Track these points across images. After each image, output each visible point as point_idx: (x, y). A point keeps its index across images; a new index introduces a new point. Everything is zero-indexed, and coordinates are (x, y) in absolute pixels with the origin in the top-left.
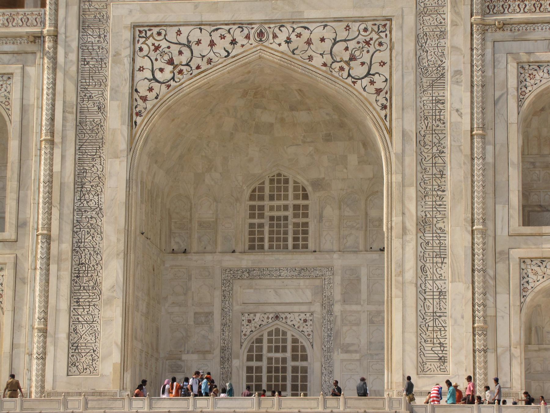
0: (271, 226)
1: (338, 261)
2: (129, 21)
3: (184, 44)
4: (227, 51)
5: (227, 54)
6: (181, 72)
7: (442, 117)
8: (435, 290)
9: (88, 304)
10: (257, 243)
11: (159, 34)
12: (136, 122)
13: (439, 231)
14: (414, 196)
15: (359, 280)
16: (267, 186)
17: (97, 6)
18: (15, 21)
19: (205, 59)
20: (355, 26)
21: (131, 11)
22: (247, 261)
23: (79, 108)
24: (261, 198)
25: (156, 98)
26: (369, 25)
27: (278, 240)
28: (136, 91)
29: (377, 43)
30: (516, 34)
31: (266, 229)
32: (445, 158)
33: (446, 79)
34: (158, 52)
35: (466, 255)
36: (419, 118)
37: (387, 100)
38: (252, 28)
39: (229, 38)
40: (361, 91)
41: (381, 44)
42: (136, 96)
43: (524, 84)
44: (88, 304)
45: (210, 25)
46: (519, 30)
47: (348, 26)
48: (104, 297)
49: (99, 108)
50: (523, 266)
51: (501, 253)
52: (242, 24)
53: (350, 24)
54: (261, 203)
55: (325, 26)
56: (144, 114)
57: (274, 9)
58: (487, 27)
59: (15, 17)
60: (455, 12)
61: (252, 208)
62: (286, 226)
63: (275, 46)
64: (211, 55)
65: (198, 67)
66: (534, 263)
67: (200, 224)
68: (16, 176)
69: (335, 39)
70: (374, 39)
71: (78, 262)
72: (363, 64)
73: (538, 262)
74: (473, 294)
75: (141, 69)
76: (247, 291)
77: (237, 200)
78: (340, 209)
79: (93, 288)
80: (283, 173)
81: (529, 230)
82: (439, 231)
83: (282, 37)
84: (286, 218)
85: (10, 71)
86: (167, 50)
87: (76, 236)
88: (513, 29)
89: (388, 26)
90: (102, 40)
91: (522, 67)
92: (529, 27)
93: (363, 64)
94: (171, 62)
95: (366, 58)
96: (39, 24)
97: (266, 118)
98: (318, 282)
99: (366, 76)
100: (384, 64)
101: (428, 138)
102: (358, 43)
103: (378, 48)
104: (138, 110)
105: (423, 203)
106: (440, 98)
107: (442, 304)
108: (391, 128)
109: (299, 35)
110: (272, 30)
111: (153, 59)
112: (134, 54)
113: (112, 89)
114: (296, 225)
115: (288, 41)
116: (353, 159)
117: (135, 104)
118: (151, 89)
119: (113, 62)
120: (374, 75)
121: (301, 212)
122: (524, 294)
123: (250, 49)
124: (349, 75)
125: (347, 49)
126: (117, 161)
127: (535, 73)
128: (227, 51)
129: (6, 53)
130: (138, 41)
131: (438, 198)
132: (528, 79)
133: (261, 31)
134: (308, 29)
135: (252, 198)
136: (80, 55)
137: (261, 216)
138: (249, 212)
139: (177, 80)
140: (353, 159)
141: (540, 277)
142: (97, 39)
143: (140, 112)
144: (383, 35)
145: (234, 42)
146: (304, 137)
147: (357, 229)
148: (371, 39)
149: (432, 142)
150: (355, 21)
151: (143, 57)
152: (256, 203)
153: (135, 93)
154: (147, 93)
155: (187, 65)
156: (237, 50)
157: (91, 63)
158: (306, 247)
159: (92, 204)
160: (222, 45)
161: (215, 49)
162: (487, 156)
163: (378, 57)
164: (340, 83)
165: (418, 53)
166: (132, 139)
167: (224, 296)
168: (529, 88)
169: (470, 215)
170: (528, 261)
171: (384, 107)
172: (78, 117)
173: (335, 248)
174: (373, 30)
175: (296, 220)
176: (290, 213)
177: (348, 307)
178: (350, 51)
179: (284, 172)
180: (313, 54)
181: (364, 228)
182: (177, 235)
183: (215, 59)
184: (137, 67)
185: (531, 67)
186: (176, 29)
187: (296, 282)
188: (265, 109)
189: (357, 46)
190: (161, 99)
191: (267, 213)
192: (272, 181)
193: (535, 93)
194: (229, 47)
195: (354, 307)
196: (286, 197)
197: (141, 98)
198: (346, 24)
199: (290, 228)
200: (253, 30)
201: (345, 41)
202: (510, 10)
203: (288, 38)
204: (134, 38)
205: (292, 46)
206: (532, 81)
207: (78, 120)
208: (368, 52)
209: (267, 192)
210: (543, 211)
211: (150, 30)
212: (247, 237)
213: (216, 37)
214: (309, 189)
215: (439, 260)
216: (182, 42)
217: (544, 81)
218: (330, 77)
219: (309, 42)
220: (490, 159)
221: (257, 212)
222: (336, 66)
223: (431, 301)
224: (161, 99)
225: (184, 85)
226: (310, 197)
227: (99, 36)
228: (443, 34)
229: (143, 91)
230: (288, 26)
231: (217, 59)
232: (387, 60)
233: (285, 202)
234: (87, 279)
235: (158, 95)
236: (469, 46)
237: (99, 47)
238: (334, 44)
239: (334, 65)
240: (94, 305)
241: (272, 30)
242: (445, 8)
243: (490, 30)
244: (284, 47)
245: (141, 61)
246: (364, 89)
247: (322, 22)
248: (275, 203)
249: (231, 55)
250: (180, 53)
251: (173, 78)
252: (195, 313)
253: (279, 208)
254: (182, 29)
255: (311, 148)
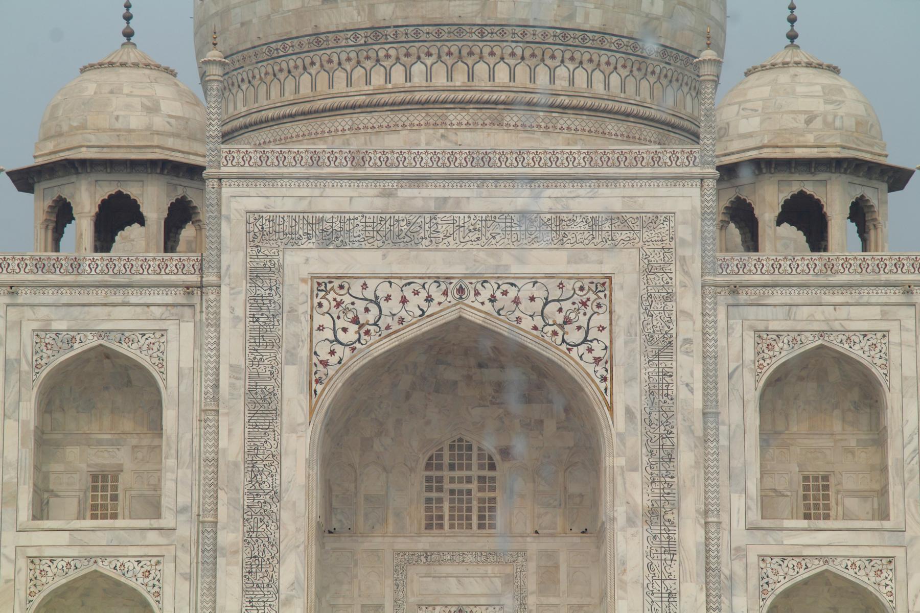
0: (452, 501)
1: (533, 546)
2: (305, 272)
3: (371, 301)
4: (421, 310)
5: (421, 313)
6: (367, 333)
7: (670, 392)
8: (664, 591)
9: (262, 604)
10: (435, 522)
11: (341, 287)
12: (315, 391)
13: (667, 524)
14: (640, 482)
15: (557, 567)
16: (446, 453)
17: (267, 253)
18: (169, 268)
19: (396, 318)
20: (569, 284)
21: (307, 260)
22: (425, 543)
23: (247, 373)
24: (440, 467)
25: (339, 363)
26: (586, 282)
27: (460, 518)
28: (315, 353)
29: (595, 304)
30: (752, 298)
31: (446, 505)
32: (675, 440)
33: (674, 348)
34: (340, 308)
35: (698, 552)
36: (644, 392)
37: (607, 370)
38: (451, 283)
39: (423, 294)
40: (578, 359)
41: (599, 306)
42: (315, 359)
43: (762, 355)
44: (262, 604)
45: (401, 278)
46: (755, 294)
47: (561, 283)
48: (282, 597)
49: (272, 373)
50: (762, 565)
51: (738, 549)
52: (438, 278)
53: (565, 282)
54: (439, 473)
55: (535, 283)
56: (325, 382)
57: (475, 261)
58: (719, 290)
59: (169, 263)
60: (684, 270)
61: (429, 479)
62: (469, 501)
63: (477, 305)
64: (403, 314)
65: (388, 327)
66: (774, 561)
67: (367, 499)
68: (173, 452)
69: (546, 299)
70: (592, 300)
71: (249, 555)
72: (579, 328)
73: (779, 560)
74: (707, 596)
75: (321, 328)
76: (425, 579)
77: (412, 470)
78: (534, 482)
79: (268, 585)
80: (465, 438)
81: (766, 523)
82: (667, 524)
83: (485, 294)
84: (469, 492)
85: (164, 328)
86: (351, 307)
87: (247, 524)
88: (749, 292)
89: (607, 284)
90: (273, 292)
91: (760, 337)
92: (768, 291)
93: (579, 328)
94: (355, 321)
95: (583, 321)
96: (197, 272)
97: (450, 374)
98: (508, 570)
99: (582, 343)
100: (604, 328)
101: (655, 416)
102: (574, 303)
103: (596, 310)
104: (318, 376)
105: (649, 491)
106: (668, 370)
107: (672, 607)
108: (612, 403)
109: (505, 293)
110: (473, 286)
111: (335, 317)
112: (312, 311)
113: (287, 351)
114: (481, 500)
115: (493, 299)
116: (550, 426)
117: (314, 369)
118: (332, 353)
119: (288, 319)
120: (591, 341)
121: (487, 484)
122: (764, 596)
123: (448, 308)
124: (563, 341)
125: (560, 310)
126: (294, 436)
127: (774, 343)
128: (421, 310)
129: (159, 305)
130: (317, 295)
131: (666, 485)
132: (766, 351)
133: (461, 287)
134: (515, 286)
135: (428, 467)
136: (248, 310)
137: (440, 489)
138: (425, 484)
139: (362, 341)
140: (550, 426)
141: (781, 578)
142: (268, 291)
143: (320, 378)
144: (601, 295)
145: (429, 299)
146: (493, 397)
147: (555, 507)
148: (588, 299)
149: (658, 420)
150: (570, 278)
151: (323, 314)
152: (434, 473)
153: (314, 357)
154: (328, 357)
155: (375, 324)
156: (434, 308)
157: (261, 320)
158: (492, 526)
159: (265, 486)
160: (416, 302)
161: (409, 306)
162: (721, 437)
163: (597, 321)
164: (554, 350)
165: (642, 317)
166: (312, 411)
167: (397, 585)
168: (768, 361)
169: (703, 506)
170: (768, 560)
171: (604, 379)
172: (247, 384)
173: (529, 530)
174: (590, 289)
175: (480, 495)
176: (474, 486)
177: (545, 600)
178: (564, 313)
179: (468, 437)
180: (522, 315)
181: (563, 506)
182: (339, 511)
183: (408, 319)
184: (315, 327)
185: (769, 337)
186: (361, 282)
187: (481, 570)
188: (449, 364)
189: (573, 307)
190: (344, 364)
191: (447, 486)
192: (452, 447)
193: (774, 366)
194: (424, 305)
195: (553, 600)
196: (469, 467)
197: (321, 362)
198: (559, 281)
199: (475, 504)
200: (452, 285)
201: (558, 301)
202: (745, 271)
203: (493, 296)
204: (312, 292)
205: (498, 305)
206: (771, 353)
207: (247, 387)
208: (585, 314)
209: (446, 460)
210: (778, 496)
211: (330, 282)
212: (423, 514)
213: (408, 293)
214: (497, 458)
215: (668, 557)
216: (368, 298)
217: (784, 353)
218: (542, 343)
219: (516, 301)
220: (723, 442)
221: (434, 484)
222: (549, 329)
223: (659, 603)
224: (344, 364)
225: (372, 348)
226: (497, 468)
227: (271, 289)
228: (670, 297)
229: (324, 356)
230: (492, 281)
231: (410, 318)
232: (606, 324)
233: (469, 473)
234: (261, 574)
235: (341, 360)
236: (700, 311)
237: (270, 301)
238: (545, 305)
239: (546, 329)
240: (270, 606)
241: (473, 286)
242: (672, 267)
243: (723, 293)
244: (488, 307)
245: (319, 320)
246: (581, 357)
247: (532, 278)
248: (457, 474)
249: (426, 314)
250: (367, 310)
251: (359, 340)
252: (363, 606)
253: (460, 480)
254: (368, 282)
255: (501, 411)
